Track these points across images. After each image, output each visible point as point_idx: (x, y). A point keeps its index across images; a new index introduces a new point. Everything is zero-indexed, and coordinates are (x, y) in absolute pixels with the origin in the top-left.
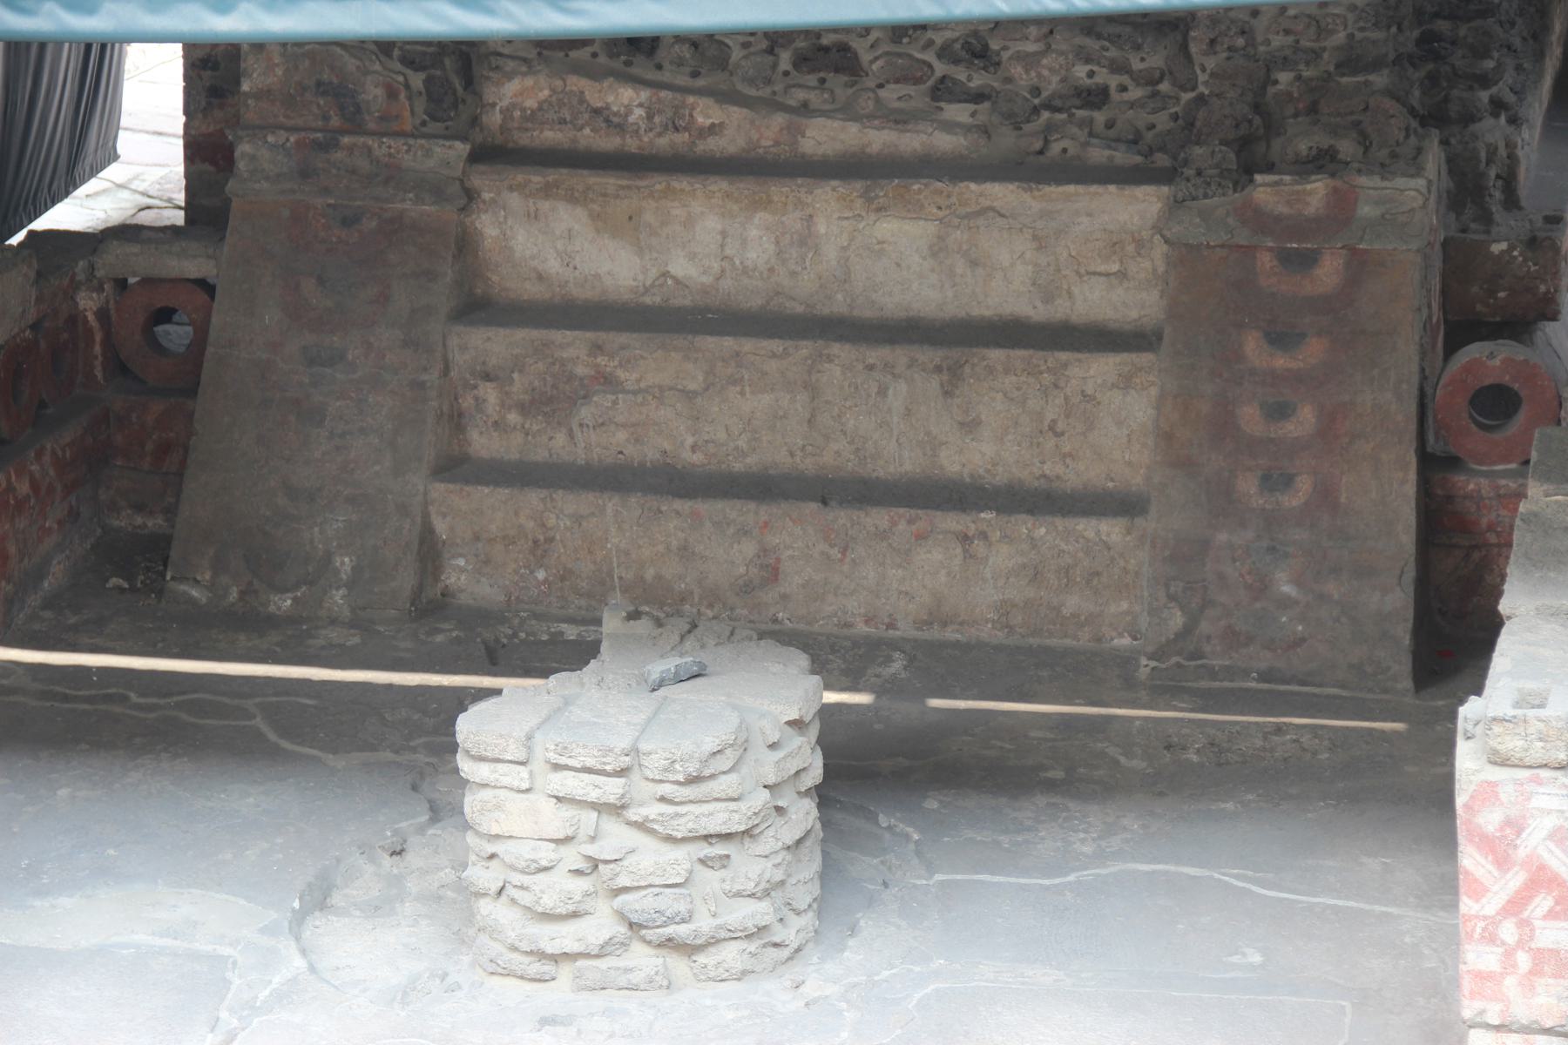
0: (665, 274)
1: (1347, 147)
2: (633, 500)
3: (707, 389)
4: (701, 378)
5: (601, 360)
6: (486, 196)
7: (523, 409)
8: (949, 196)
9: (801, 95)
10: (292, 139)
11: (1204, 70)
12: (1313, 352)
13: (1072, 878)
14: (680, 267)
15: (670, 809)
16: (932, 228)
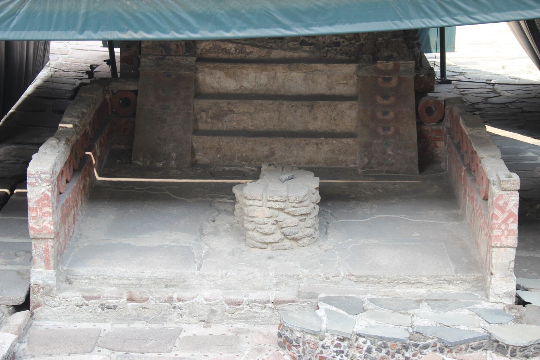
0: (242, 86)
1: (395, 54)
3: (255, 112)
4: (253, 110)
5: (230, 106)
6: (200, 69)
7: (212, 118)
8: (308, 67)
9: (271, 45)
10: (154, 57)
11: (362, 38)
12: (392, 100)
13: (369, 219)
14: (245, 84)
15: (295, 209)
16: (304, 74)
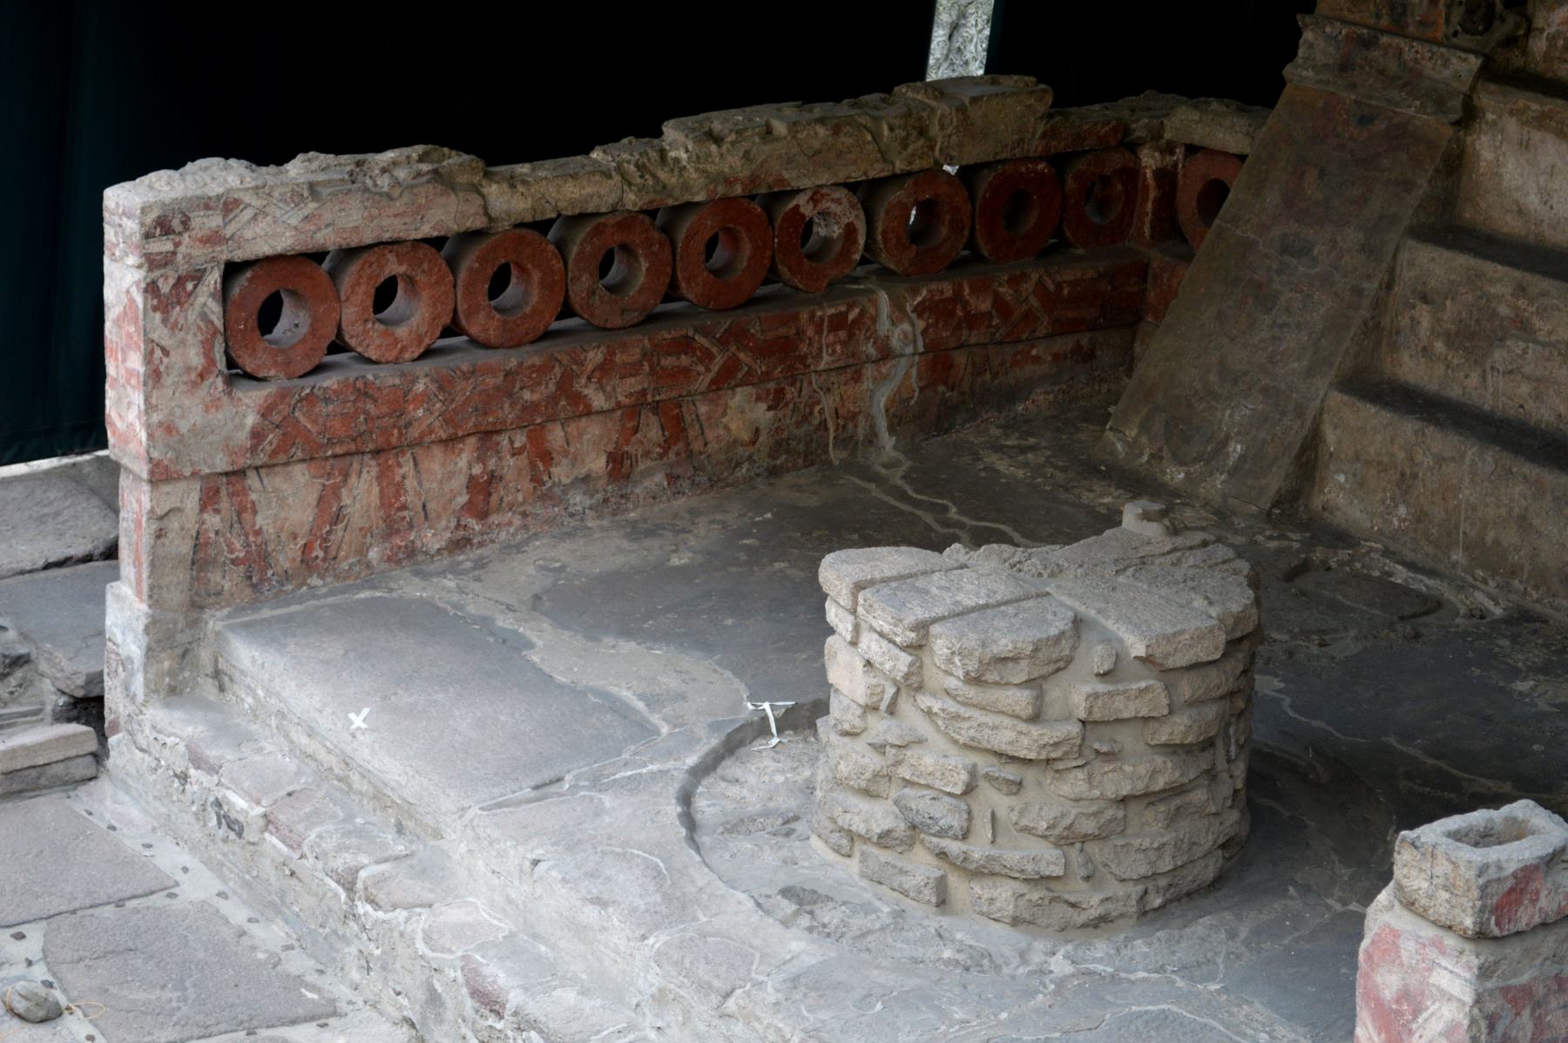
2: (1489, 456)
5: (1522, 303)
6: (1490, 116)
7: (1449, 339)
10: (1344, 32)
15: (953, 707)
